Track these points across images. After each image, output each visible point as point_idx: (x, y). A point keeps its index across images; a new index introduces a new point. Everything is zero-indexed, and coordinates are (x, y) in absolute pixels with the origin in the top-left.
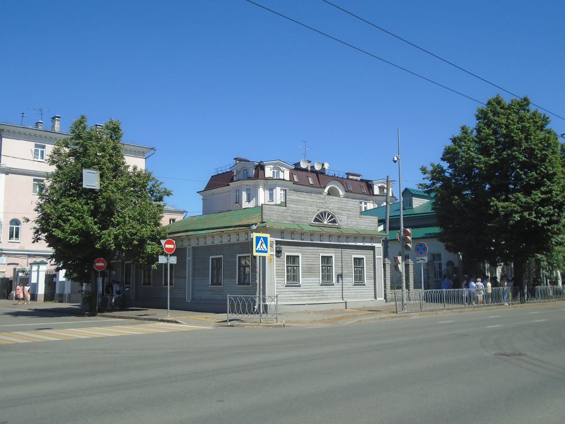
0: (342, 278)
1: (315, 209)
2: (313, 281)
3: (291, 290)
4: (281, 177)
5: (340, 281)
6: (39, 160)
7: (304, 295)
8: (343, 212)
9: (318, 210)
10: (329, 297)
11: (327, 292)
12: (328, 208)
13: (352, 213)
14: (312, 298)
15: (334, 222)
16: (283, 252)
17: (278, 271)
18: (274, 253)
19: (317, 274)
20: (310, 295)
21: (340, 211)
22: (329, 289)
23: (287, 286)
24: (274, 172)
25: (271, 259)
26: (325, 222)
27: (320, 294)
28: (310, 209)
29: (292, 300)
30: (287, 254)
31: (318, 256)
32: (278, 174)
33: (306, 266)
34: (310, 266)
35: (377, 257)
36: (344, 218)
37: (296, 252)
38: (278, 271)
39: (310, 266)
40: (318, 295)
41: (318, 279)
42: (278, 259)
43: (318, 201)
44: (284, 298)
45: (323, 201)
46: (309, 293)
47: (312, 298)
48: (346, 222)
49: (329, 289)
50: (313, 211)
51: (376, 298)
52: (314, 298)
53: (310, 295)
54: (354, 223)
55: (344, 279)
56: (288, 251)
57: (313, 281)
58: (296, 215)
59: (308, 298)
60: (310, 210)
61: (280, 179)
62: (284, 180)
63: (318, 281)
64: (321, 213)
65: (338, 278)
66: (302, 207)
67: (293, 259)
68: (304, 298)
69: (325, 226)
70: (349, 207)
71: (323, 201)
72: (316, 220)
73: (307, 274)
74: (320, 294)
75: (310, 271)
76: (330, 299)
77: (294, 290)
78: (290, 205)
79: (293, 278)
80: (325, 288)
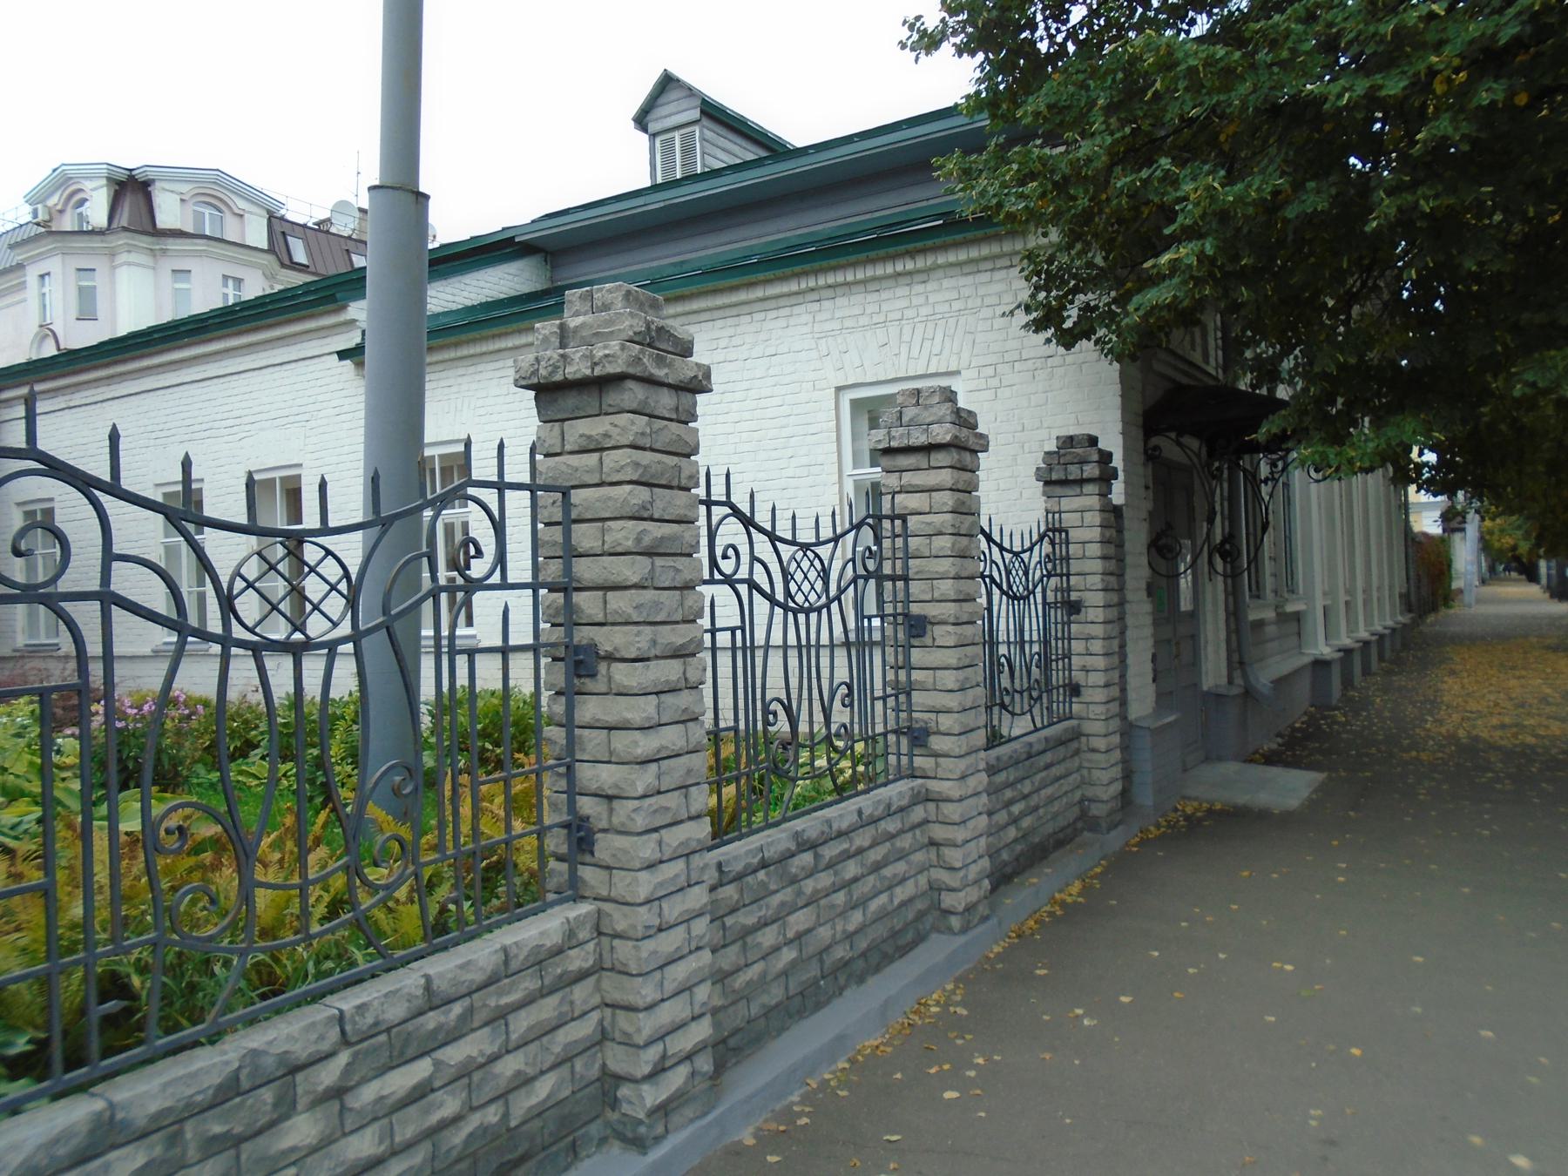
24: (199, 217)
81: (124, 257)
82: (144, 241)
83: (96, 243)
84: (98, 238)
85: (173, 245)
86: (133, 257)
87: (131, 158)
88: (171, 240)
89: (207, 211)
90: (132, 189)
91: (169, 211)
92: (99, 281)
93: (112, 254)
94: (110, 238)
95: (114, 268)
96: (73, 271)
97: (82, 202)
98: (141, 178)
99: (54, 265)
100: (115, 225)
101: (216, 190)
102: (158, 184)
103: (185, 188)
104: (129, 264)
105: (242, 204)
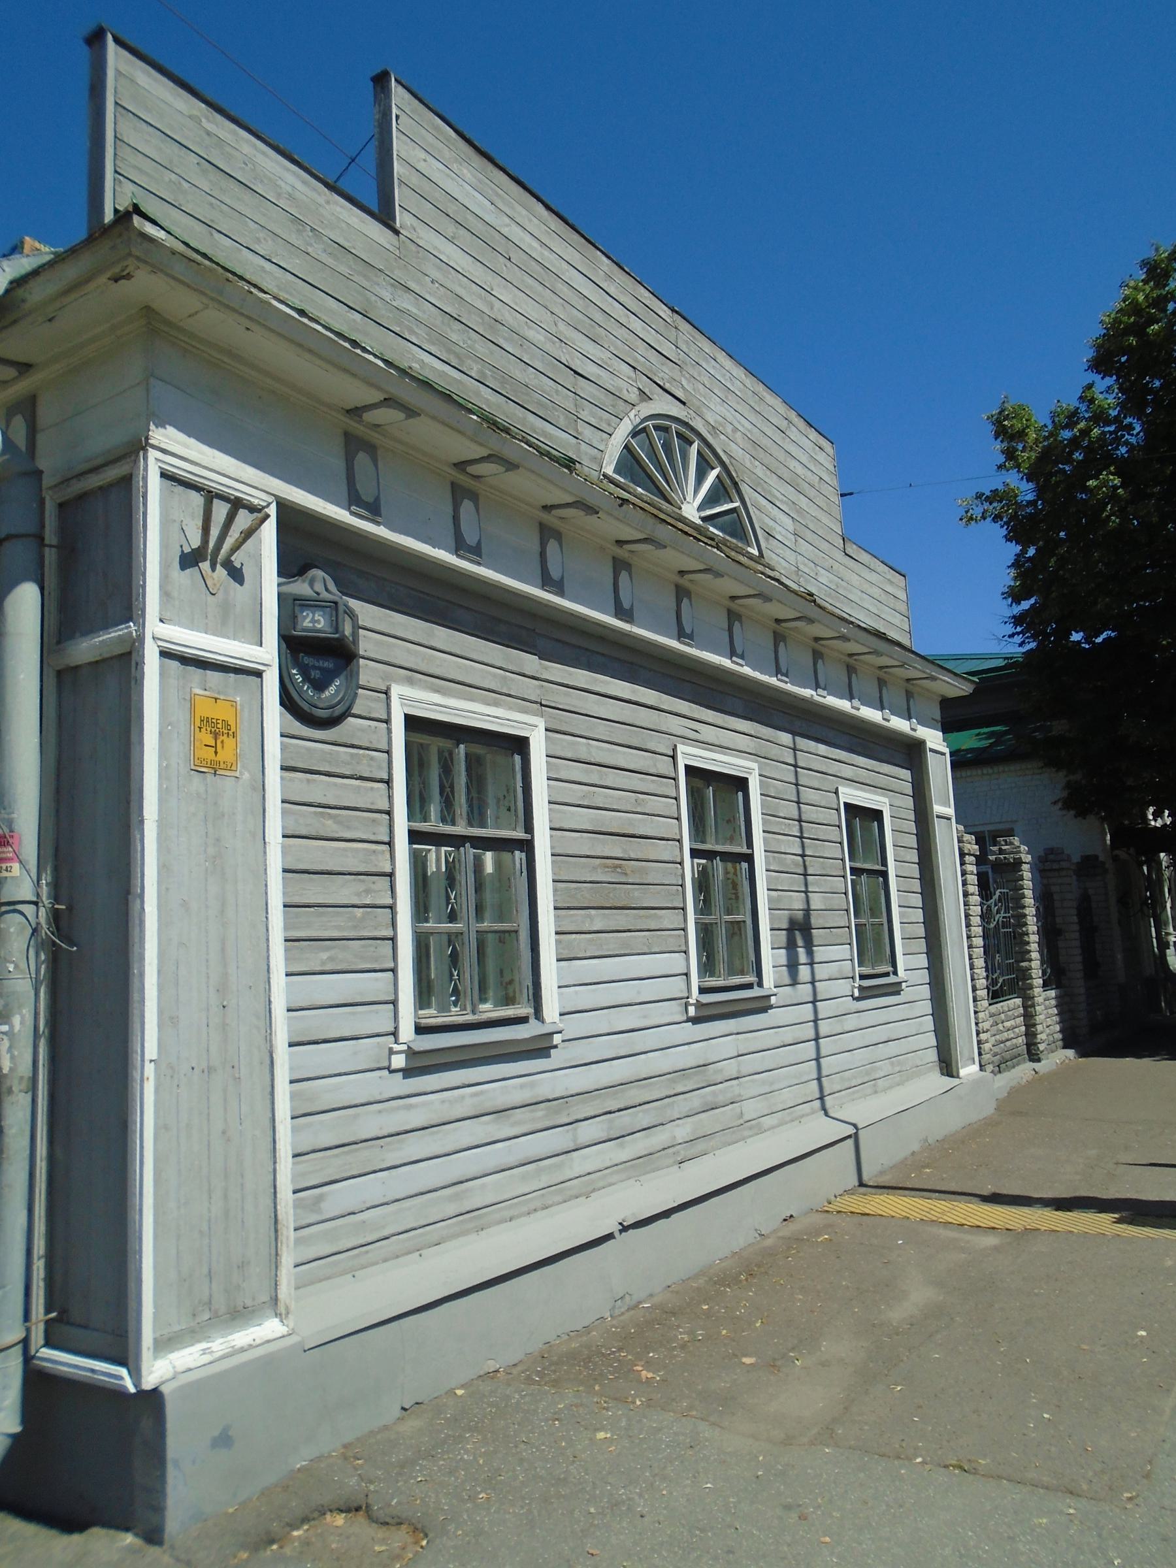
0: (809, 946)
3: (467, 1101)
5: (804, 972)
7: (589, 1131)
10: (751, 1109)
11: (730, 1068)
16: (367, 673)
17: (315, 890)
18: (266, 653)
19: (670, 919)
20: (625, 1120)
23: (419, 1065)
25: (218, 730)
27: (695, 1101)
30: (409, 698)
31: (664, 765)
33: (584, 844)
34: (613, 847)
38: (315, 890)
39: (613, 847)
40: (682, 1105)
42: (316, 748)
44: (409, 1213)
46: (619, 1108)
52: (659, 1138)
55: (820, 953)
56: (417, 675)
63: (676, 987)
65: (791, 946)
67: (464, 768)
68: (581, 1163)
73: (598, 920)
74: (695, 1101)
75: (609, 900)
77: (498, 1095)
79: (476, 964)
80: (723, 1041)
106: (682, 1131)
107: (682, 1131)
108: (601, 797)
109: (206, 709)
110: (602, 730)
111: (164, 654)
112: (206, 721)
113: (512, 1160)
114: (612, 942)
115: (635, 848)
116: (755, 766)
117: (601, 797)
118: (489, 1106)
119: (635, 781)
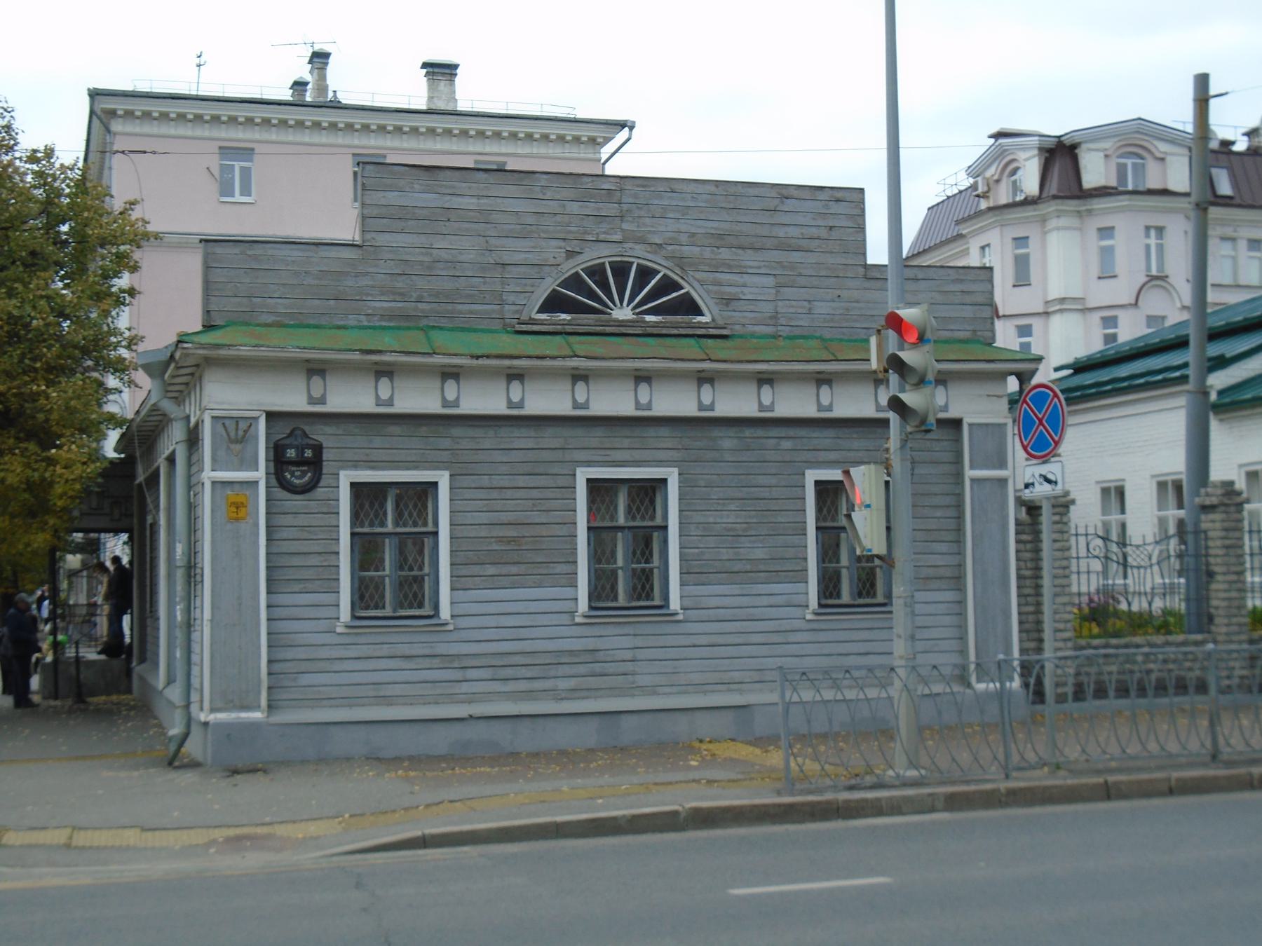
1: (552, 250)
2: (533, 607)
4: (1153, 184)
6: (238, 198)
8: (749, 259)
9: (571, 254)
11: (628, 655)
12: (641, 240)
13: (812, 258)
14: (523, 685)
15: (689, 306)
18: (260, 474)
21: (725, 254)
22: (639, 642)
25: (238, 506)
26: (623, 313)
28: (515, 251)
29: (388, 700)
32: (1140, 170)
35: (970, 473)
36: (756, 287)
37: (414, 465)
41: (568, 592)
43: (574, 208)
45: (611, 209)
47: (523, 685)
48: (768, 308)
49: (639, 642)
50: (533, 258)
51: (964, 680)
53: (509, 672)
54: (822, 309)
57: (533, 607)
58: (421, 283)
59: (497, 687)
60: (519, 258)
61: (1151, 192)
62: (1165, 192)
63: (567, 606)
64: (597, 272)
66: (466, 243)
68: (465, 688)
69: (622, 332)
70: (793, 232)
71: (611, 209)
72: (554, 303)
74: (582, 669)
76: (653, 691)
78: (382, 239)
80: (616, 639)
81: (1053, 223)
82: (1072, 205)
83: (1029, 212)
84: (1030, 207)
85: (1098, 204)
86: (1063, 221)
87: (1056, 126)
88: (1096, 200)
89: (1129, 162)
90: (1061, 154)
91: (1094, 171)
92: (1033, 249)
93: (1043, 220)
94: (1041, 206)
95: (1045, 233)
96: (1010, 241)
97: (1014, 172)
98: (1067, 141)
99: (993, 237)
100: (1044, 195)
101: (1136, 139)
102: (1084, 146)
103: (1107, 144)
104: (1058, 229)
105: (1163, 147)
106: (563, 684)
107: (563, 684)
108: (498, 505)
109: (232, 499)
110: (504, 469)
111: (213, 483)
112: (233, 504)
113: (415, 679)
114: (505, 581)
115: (526, 531)
116: (676, 471)
117: (498, 505)
118: (399, 654)
119: (535, 494)
